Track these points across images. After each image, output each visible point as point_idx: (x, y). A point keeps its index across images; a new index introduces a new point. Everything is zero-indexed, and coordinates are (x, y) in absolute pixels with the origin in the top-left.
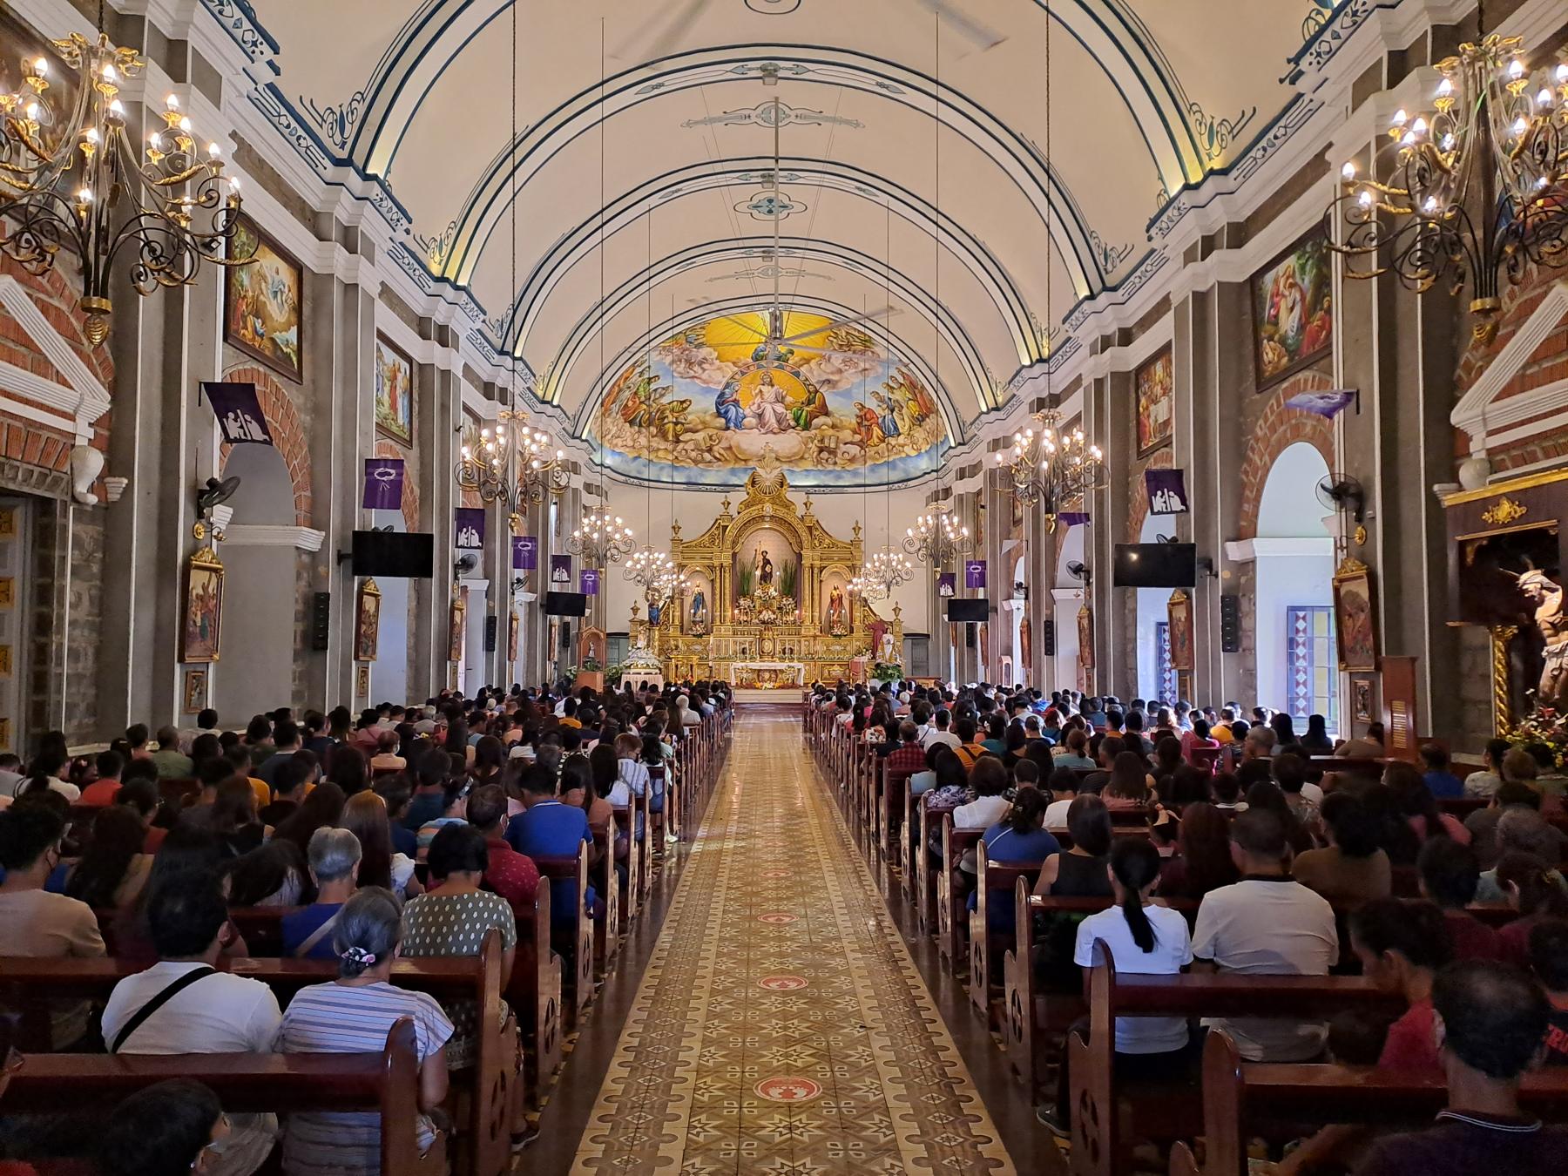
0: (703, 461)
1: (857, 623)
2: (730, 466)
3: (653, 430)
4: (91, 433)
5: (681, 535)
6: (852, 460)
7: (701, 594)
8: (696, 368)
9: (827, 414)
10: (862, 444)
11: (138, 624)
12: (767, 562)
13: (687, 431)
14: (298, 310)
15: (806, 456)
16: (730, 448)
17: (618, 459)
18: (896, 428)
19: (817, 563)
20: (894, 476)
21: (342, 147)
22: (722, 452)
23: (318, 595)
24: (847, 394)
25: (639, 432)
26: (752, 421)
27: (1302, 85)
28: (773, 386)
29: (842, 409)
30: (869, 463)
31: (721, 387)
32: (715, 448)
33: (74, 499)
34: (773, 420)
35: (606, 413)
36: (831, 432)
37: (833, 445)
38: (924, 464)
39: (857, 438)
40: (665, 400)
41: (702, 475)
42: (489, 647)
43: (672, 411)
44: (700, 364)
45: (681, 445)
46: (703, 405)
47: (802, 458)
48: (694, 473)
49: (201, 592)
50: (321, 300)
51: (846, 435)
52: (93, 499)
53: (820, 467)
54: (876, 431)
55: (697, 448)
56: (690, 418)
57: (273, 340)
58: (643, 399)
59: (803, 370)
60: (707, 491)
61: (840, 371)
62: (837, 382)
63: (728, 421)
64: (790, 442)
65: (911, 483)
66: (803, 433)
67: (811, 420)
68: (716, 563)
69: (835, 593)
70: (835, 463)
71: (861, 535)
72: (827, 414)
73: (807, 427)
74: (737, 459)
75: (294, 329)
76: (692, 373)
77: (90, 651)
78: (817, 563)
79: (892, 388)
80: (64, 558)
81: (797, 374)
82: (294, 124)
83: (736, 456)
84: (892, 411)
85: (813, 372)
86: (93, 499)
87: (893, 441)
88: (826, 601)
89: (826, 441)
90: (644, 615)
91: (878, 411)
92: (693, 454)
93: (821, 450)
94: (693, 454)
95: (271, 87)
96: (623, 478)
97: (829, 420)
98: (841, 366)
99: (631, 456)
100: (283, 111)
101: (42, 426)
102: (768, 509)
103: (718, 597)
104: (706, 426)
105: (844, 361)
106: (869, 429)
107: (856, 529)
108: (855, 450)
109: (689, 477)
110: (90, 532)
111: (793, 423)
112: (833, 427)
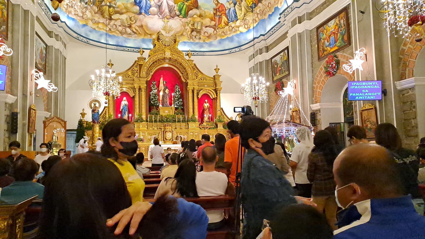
0: (126, 33)
2: (142, 37)
6: (209, 37)
9: (197, 7)
10: (215, 27)
13: (117, 12)
15: (184, 34)
16: (142, 26)
18: (236, 16)
19: (196, 87)
22: (137, 28)
26: (154, 9)
30: (219, 38)
32: (133, 26)
34: (167, 10)
36: (199, 19)
37: (199, 28)
38: (250, 36)
39: (213, 23)
41: (125, 42)
45: (112, 22)
47: (182, 35)
48: (121, 40)
51: (207, 21)
53: (191, 40)
54: (224, 18)
55: (123, 25)
60: (128, 51)
65: (243, 47)
66: (184, 20)
67: (188, 11)
68: (136, 86)
70: (200, 38)
72: (197, 7)
73: (186, 15)
74: (146, 34)
78: (196, 87)
84: (235, 4)
87: (232, 24)
89: (196, 25)
92: (120, 28)
93: (192, 31)
94: (120, 28)
96: (75, 35)
99: (81, 23)
102: (168, 54)
104: (128, 11)
106: (220, 18)
108: (211, 31)
109: (117, 42)
111: (178, 13)
112: (200, 16)
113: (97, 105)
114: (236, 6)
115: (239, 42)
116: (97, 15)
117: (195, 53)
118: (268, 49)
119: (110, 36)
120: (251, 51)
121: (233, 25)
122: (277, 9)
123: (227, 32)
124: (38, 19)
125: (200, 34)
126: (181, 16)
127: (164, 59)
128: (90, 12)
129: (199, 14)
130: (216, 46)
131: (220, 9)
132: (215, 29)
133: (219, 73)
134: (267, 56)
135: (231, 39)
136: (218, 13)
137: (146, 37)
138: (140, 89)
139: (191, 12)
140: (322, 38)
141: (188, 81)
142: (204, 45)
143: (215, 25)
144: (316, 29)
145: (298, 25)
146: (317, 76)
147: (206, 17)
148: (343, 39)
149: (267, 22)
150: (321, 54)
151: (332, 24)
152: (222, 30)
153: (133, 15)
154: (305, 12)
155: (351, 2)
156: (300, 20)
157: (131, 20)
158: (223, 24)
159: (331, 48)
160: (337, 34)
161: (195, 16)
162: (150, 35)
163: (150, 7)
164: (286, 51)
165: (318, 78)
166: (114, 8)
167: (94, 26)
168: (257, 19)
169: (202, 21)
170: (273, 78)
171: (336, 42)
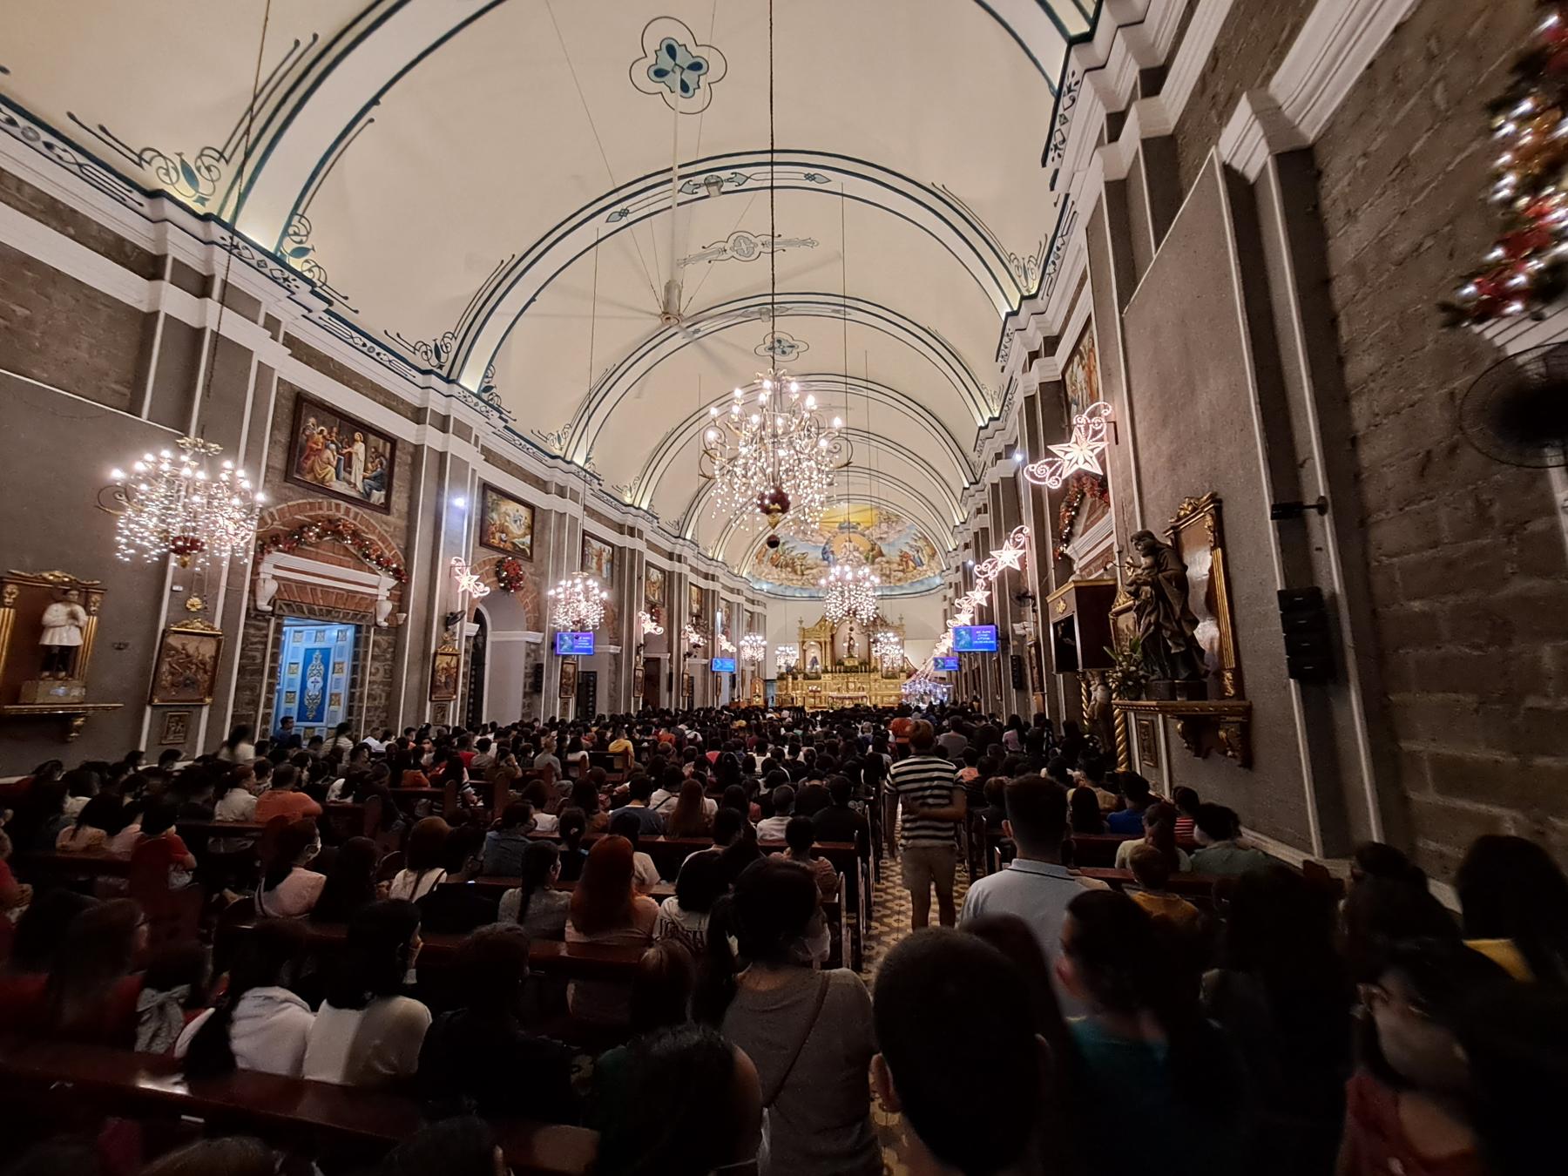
3: (789, 569)
4: (388, 594)
6: (900, 580)
7: (815, 658)
10: (903, 571)
11: (408, 679)
14: (531, 528)
17: (770, 586)
20: (924, 588)
21: (561, 449)
23: (538, 665)
33: (376, 624)
35: (760, 562)
40: (793, 554)
42: (670, 689)
45: (805, 577)
49: (445, 666)
50: (545, 523)
51: (895, 566)
52: (386, 624)
54: (911, 563)
57: (513, 544)
61: (886, 533)
68: (822, 640)
71: (903, 622)
75: (529, 537)
77: (384, 695)
80: (367, 652)
82: (523, 443)
86: (386, 624)
91: (910, 553)
95: (506, 427)
97: (884, 559)
99: (778, 583)
100: (516, 438)
101: (358, 592)
104: (817, 566)
106: (907, 562)
107: (901, 619)
108: (900, 574)
110: (384, 640)
112: (887, 562)
115: (929, 585)
133: (903, 622)
135: (921, 582)
138: (825, 643)
158: (911, 568)
167: (789, 583)
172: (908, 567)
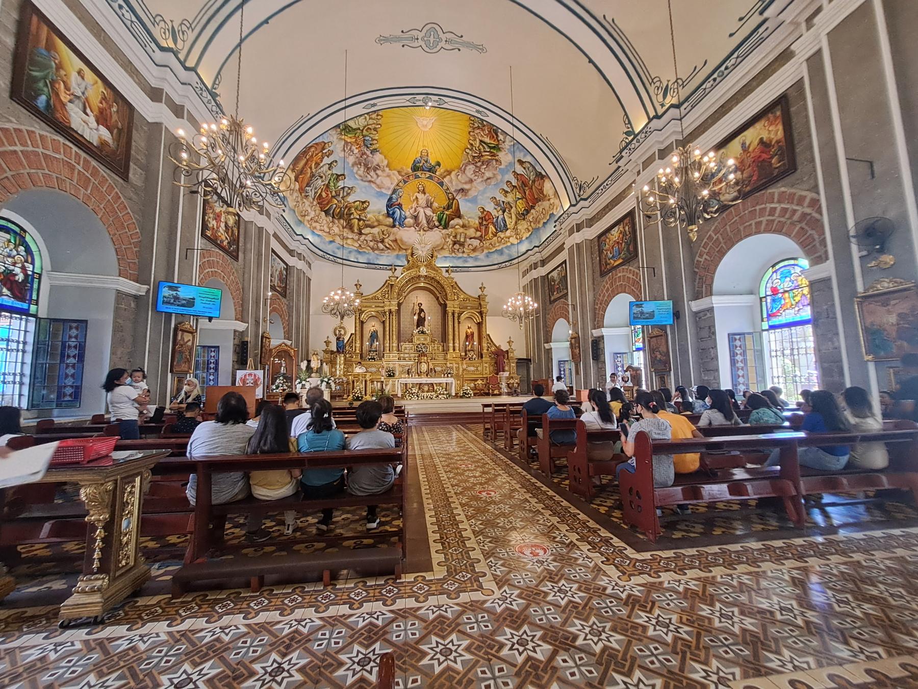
0: (378, 249)
1: (485, 351)
2: (396, 253)
5: (361, 290)
6: (474, 250)
7: (376, 332)
8: (372, 173)
9: (460, 217)
10: (480, 239)
12: (422, 310)
13: (367, 226)
15: (445, 247)
16: (396, 241)
18: (505, 225)
19: (457, 310)
24: (474, 200)
25: (333, 222)
26: (410, 221)
27: (620, 163)
28: (425, 193)
29: (470, 211)
30: (486, 251)
31: (390, 193)
32: (386, 240)
34: (424, 222)
36: (461, 230)
37: (462, 240)
38: (523, 248)
39: (479, 234)
40: (350, 199)
43: (356, 209)
44: (375, 169)
45: (363, 237)
46: (378, 207)
47: (442, 248)
51: (471, 232)
53: (453, 255)
54: (492, 228)
55: (374, 240)
56: (369, 216)
58: (334, 194)
59: (446, 180)
60: (380, 269)
62: (468, 190)
63: (394, 220)
64: (436, 236)
66: (444, 231)
68: (387, 309)
69: (469, 331)
70: (464, 252)
72: (460, 217)
73: (446, 227)
74: (400, 249)
76: (369, 178)
79: (507, 192)
81: (441, 184)
83: (398, 244)
84: (504, 212)
85: (453, 182)
88: (463, 336)
89: (458, 237)
90: (334, 347)
91: (494, 213)
92: (371, 244)
93: (455, 243)
96: (321, 253)
97: (460, 222)
98: (472, 177)
99: (328, 239)
102: (423, 271)
103: (387, 333)
104: (380, 223)
105: (475, 172)
106: (487, 227)
108: (476, 243)
111: (437, 224)
112: (464, 226)
113: (342, 332)
114: (505, 213)
115: (509, 255)
116: (345, 230)
117: (458, 269)
118: (544, 263)
119: (360, 252)
120: (525, 266)
121: (502, 236)
122: (552, 215)
123: (495, 244)
124: (276, 236)
125: (464, 247)
126: (441, 227)
127: (419, 276)
128: (338, 226)
129: (461, 223)
130: (483, 260)
131: (487, 217)
132: (481, 241)
134: (542, 271)
135: (501, 252)
136: (484, 223)
137: (400, 253)
139: (452, 222)
140: (605, 248)
141: (447, 302)
142: (469, 259)
143: (481, 236)
144: (596, 240)
145: (576, 234)
146: (600, 295)
147: (469, 227)
148: (628, 249)
149: (541, 231)
150: (603, 268)
151: (615, 232)
152: (490, 241)
153: (386, 228)
154: (584, 218)
155: (636, 205)
156: (579, 227)
157: (383, 234)
159: (615, 261)
160: (621, 244)
161: (457, 227)
162: (406, 250)
163: (406, 218)
164: (564, 265)
165: (601, 298)
166: (364, 221)
168: (530, 228)
169: (466, 232)
170: (550, 297)
171: (620, 254)
172: (487, 232)
